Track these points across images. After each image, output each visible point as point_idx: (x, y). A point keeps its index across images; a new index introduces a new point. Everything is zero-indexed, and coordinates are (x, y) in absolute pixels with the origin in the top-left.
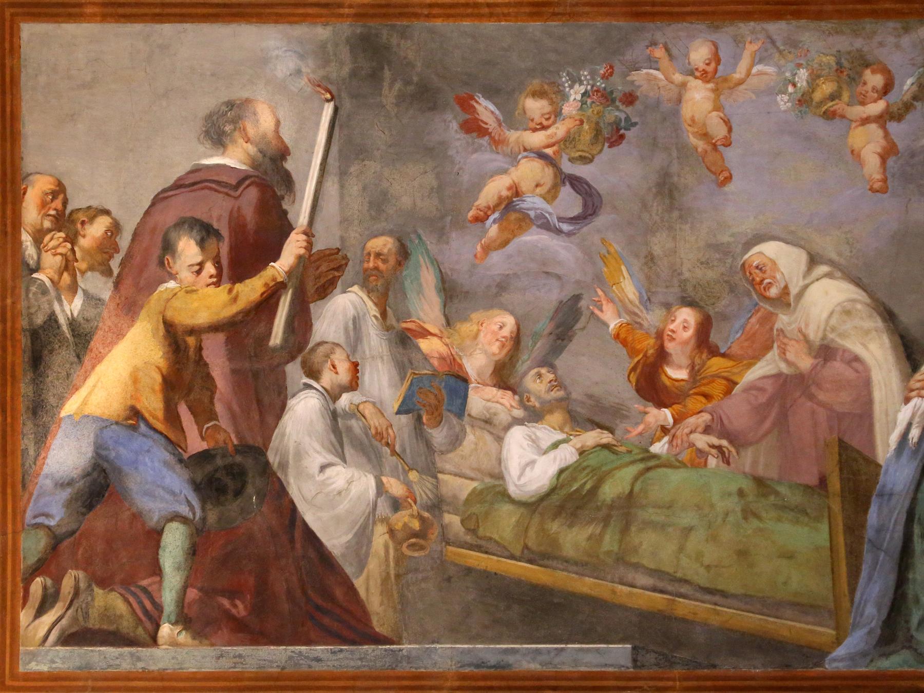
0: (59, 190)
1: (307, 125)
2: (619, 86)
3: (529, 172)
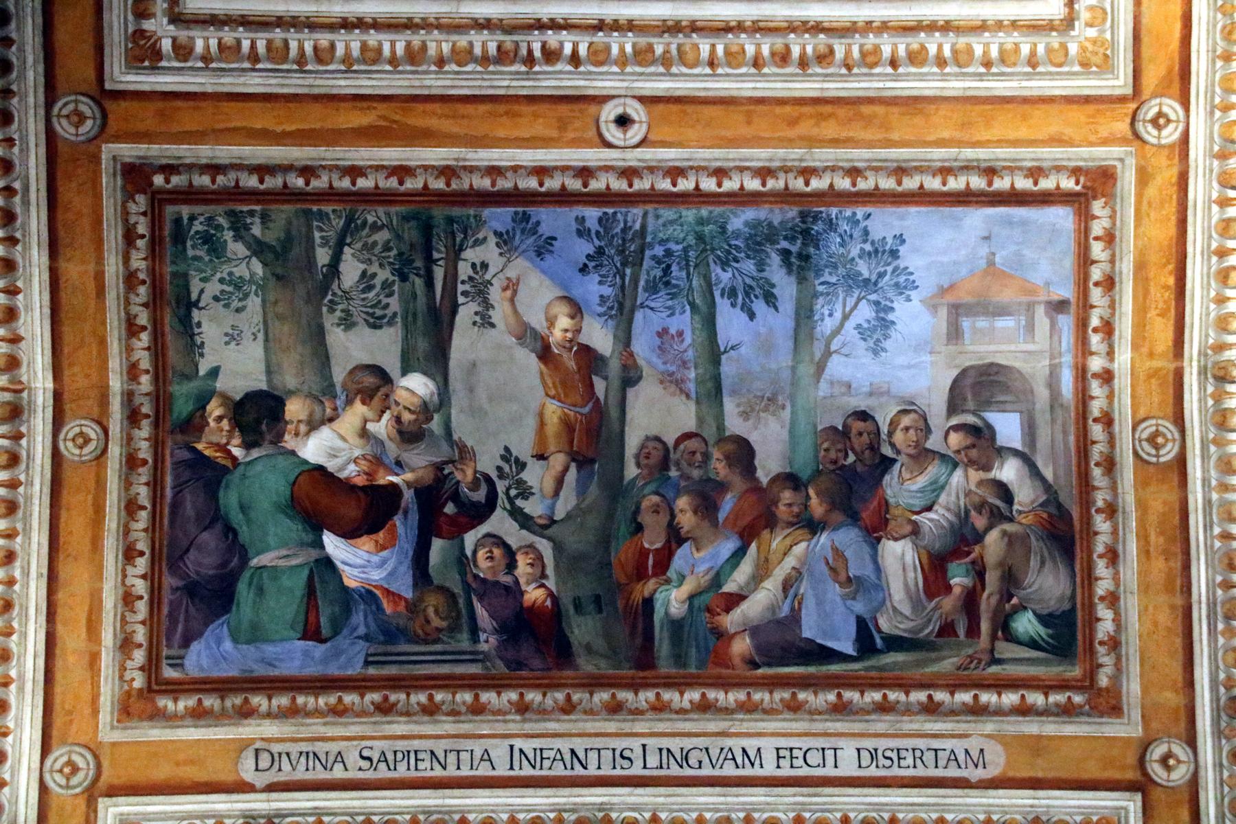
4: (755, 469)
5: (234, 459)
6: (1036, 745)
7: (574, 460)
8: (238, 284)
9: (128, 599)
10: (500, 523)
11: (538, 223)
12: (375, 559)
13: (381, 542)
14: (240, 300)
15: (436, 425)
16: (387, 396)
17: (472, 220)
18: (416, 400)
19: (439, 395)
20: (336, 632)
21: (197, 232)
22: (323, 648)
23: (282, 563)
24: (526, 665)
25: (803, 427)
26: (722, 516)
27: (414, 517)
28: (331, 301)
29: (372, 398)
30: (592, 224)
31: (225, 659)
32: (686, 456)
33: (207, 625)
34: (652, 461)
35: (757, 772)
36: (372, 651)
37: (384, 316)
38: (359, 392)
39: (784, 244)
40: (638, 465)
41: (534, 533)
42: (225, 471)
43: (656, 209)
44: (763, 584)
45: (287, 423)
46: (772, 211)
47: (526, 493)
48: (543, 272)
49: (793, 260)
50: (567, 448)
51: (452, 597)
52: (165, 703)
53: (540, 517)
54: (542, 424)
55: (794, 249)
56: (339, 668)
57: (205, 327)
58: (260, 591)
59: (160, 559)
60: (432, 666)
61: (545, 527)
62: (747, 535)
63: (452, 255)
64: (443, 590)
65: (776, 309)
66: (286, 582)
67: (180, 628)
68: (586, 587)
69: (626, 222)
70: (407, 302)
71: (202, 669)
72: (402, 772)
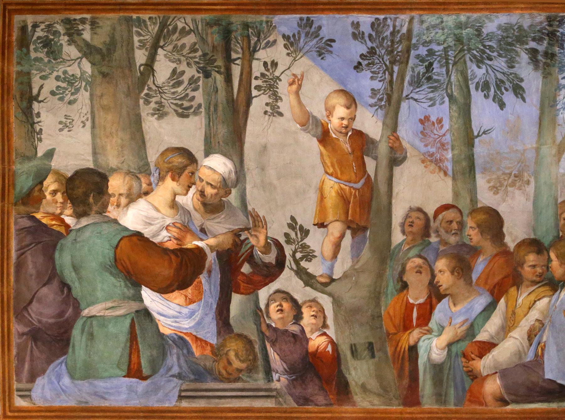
4: (504, 235)
5: (67, 226)
7: (349, 228)
8: (70, 80)
10: (288, 281)
11: (320, 28)
12: (185, 311)
13: (190, 296)
14: (72, 94)
15: (233, 198)
16: (193, 173)
17: (264, 25)
18: (216, 177)
19: (236, 172)
20: (154, 371)
21: (39, 38)
22: (145, 383)
23: (108, 313)
24: (312, 401)
25: (545, 198)
26: (475, 276)
27: (217, 276)
28: (147, 95)
29: (180, 175)
30: (366, 29)
31: (63, 390)
32: (444, 224)
33: (49, 362)
34: (415, 229)
36: (184, 387)
37: (191, 107)
38: (170, 170)
39: (533, 45)
40: (403, 232)
41: (315, 289)
42: (59, 236)
43: (421, 16)
44: (511, 334)
45: (110, 196)
46: (522, 16)
47: (309, 256)
48: (323, 68)
49: (540, 58)
50: (343, 218)
51: (250, 342)
53: (321, 276)
54: (322, 198)
55: (541, 48)
56: (157, 401)
57: (43, 115)
58: (91, 336)
59: (8, 311)
60: (234, 400)
61: (326, 285)
62: (497, 292)
63: (247, 53)
64: (240, 336)
65: (524, 100)
66: (112, 329)
67: (27, 366)
68: (361, 336)
69: (394, 27)
70: (209, 95)
71: (46, 400)
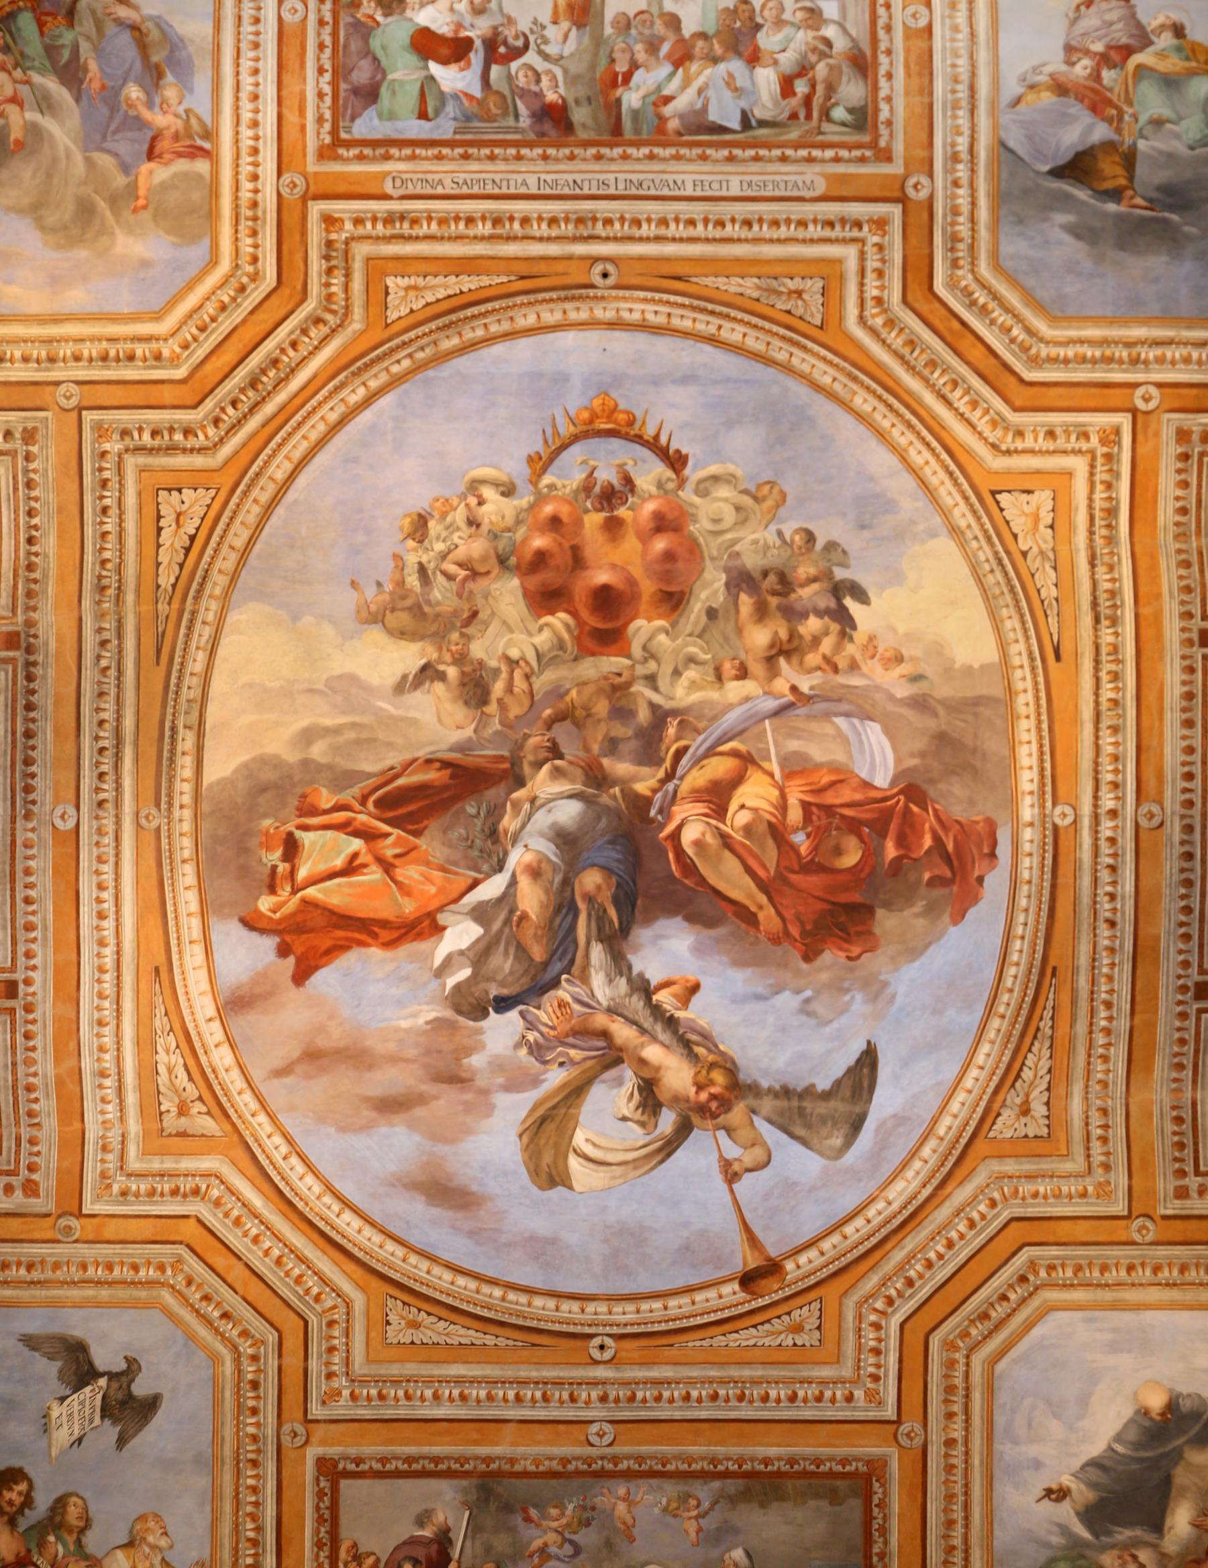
0: (355, 1545)
1: (459, 1520)
2: (588, 1503)
3: (551, 1537)
6: (844, 179)
9: (321, 95)
20: (437, 113)
35: (682, 193)
52: (342, 151)
58: (394, 93)
68: (581, 91)
72: (476, 190)
